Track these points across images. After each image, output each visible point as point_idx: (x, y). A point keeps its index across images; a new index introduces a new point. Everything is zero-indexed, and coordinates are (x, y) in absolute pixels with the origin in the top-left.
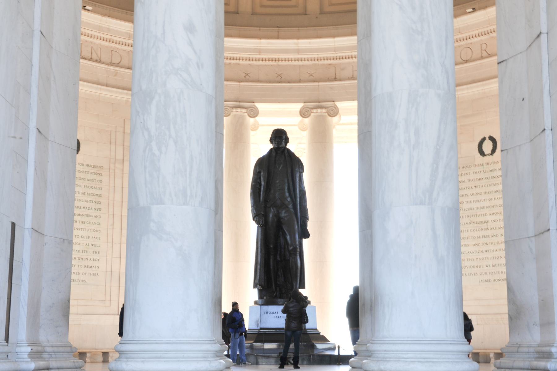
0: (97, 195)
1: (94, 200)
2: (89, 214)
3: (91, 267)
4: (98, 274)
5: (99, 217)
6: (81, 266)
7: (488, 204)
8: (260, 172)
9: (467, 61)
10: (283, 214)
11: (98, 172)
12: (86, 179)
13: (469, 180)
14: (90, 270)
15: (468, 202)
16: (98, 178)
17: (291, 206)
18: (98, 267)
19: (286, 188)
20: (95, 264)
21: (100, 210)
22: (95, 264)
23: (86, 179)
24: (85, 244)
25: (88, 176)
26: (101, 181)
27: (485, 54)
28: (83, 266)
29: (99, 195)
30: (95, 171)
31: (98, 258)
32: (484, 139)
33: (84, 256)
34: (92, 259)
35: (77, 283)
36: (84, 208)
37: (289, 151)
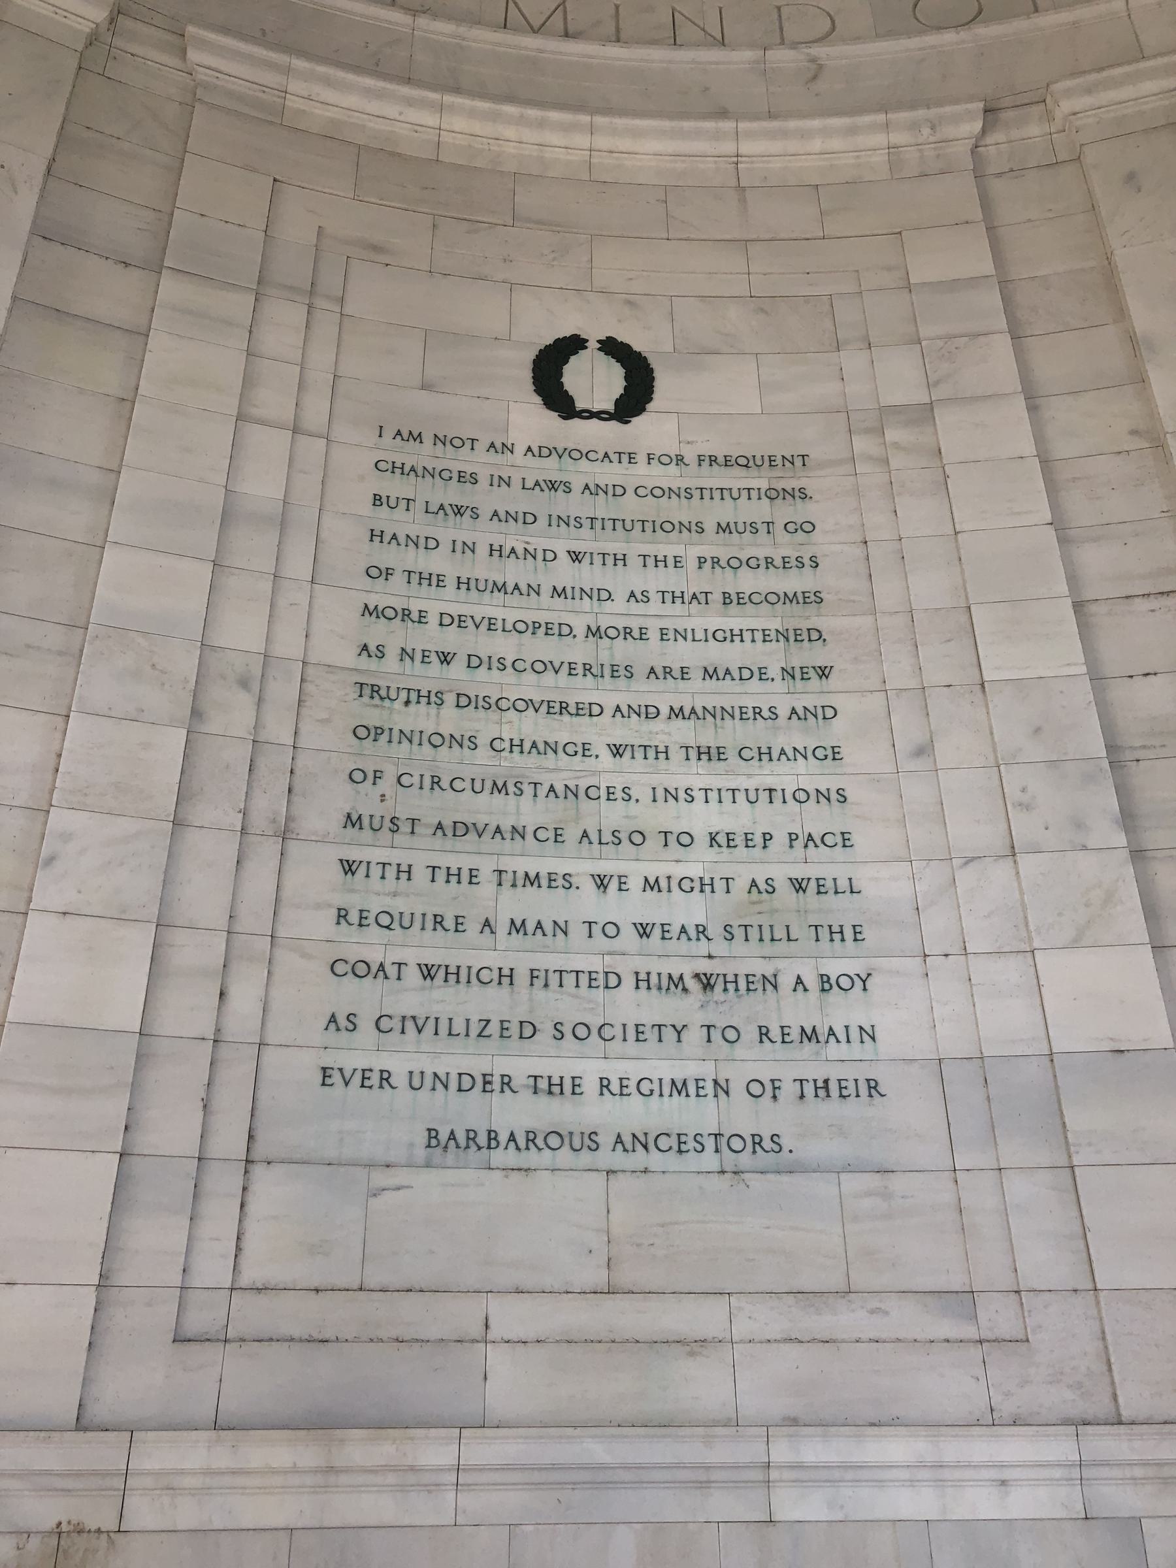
0: (790, 599)
1: (774, 624)
2: (750, 703)
3: (809, 1035)
4: (873, 1086)
5: (827, 714)
6: (731, 1035)
11: (780, 485)
12: (710, 526)
14: (808, 1064)
16: (785, 512)
18: (869, 1034)
20: (843, 1012)
21: (823, 673)
22: (843, 1012)
23: (710, 526)
24: (740, 885)
25: (715, 512)
26: (807, 528)
28: (750, 1033)
30: (764, 484)
31: (853, 967)
33: (748, 960)
34: (811, 981)
35: (710, 1160)
36: (709, 673)
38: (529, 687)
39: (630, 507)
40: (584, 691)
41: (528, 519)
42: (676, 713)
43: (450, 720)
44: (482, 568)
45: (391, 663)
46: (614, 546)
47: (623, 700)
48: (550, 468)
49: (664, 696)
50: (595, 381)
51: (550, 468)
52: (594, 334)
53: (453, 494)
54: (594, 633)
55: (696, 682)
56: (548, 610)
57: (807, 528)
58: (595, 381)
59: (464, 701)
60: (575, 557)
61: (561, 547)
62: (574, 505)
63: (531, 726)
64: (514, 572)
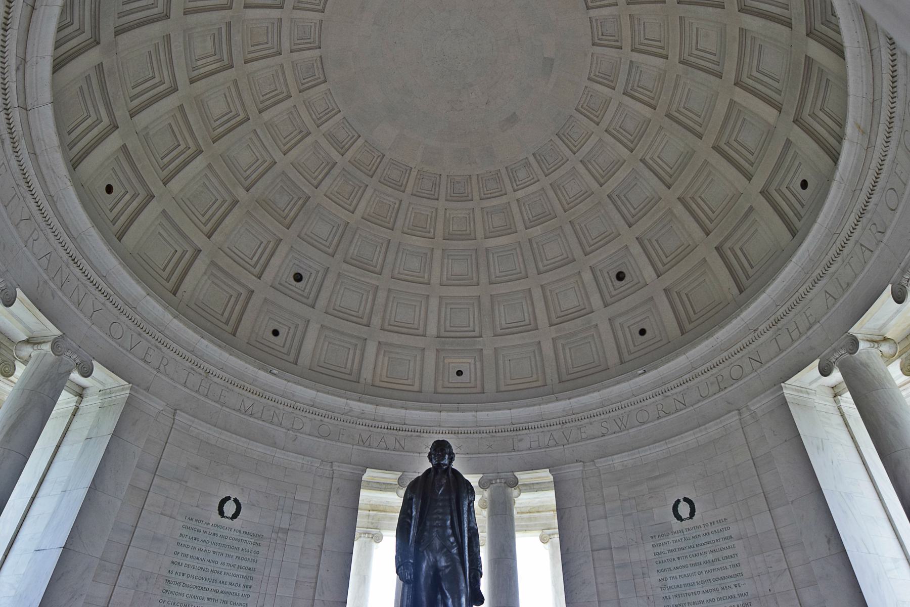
1: (245, 574)
5: (248, 596)
7: (698, 578)
8: (411, 499)
9: (644, 423)
10: (443, 563)
13: (670, 551)
15: (673, 578)
16: (256, 548)
17: (455, 551)
19: (449, 522)
26: (257, 553)
27: (662, 414)
29: (253, 570)
32: (678, 501)
36: (230, 584)
37: (454, 471)
38: (197, 583)
39: (227, 542)
40: (206, 585)
41: (208, 542)
42: (222, 592)
43: (181, 589)
44: (197, 554)
45: (173, 575)
46: (221, 551)
47: (213, 588)
48: (215, 530)
49: (221, 587)
50: (230, 508)
51: (215, 530)
52: (233, 497)
53: (195, 534)
54: (212, 571)
55: (227, 586)
56: (206, 565)
57: (257, 553)
58: (230, 508)
59: (185, 585)
60: (214, 552)
61: (212, 549)
62: (217, 540)
63: (195, 592)
64: (202, 555)
